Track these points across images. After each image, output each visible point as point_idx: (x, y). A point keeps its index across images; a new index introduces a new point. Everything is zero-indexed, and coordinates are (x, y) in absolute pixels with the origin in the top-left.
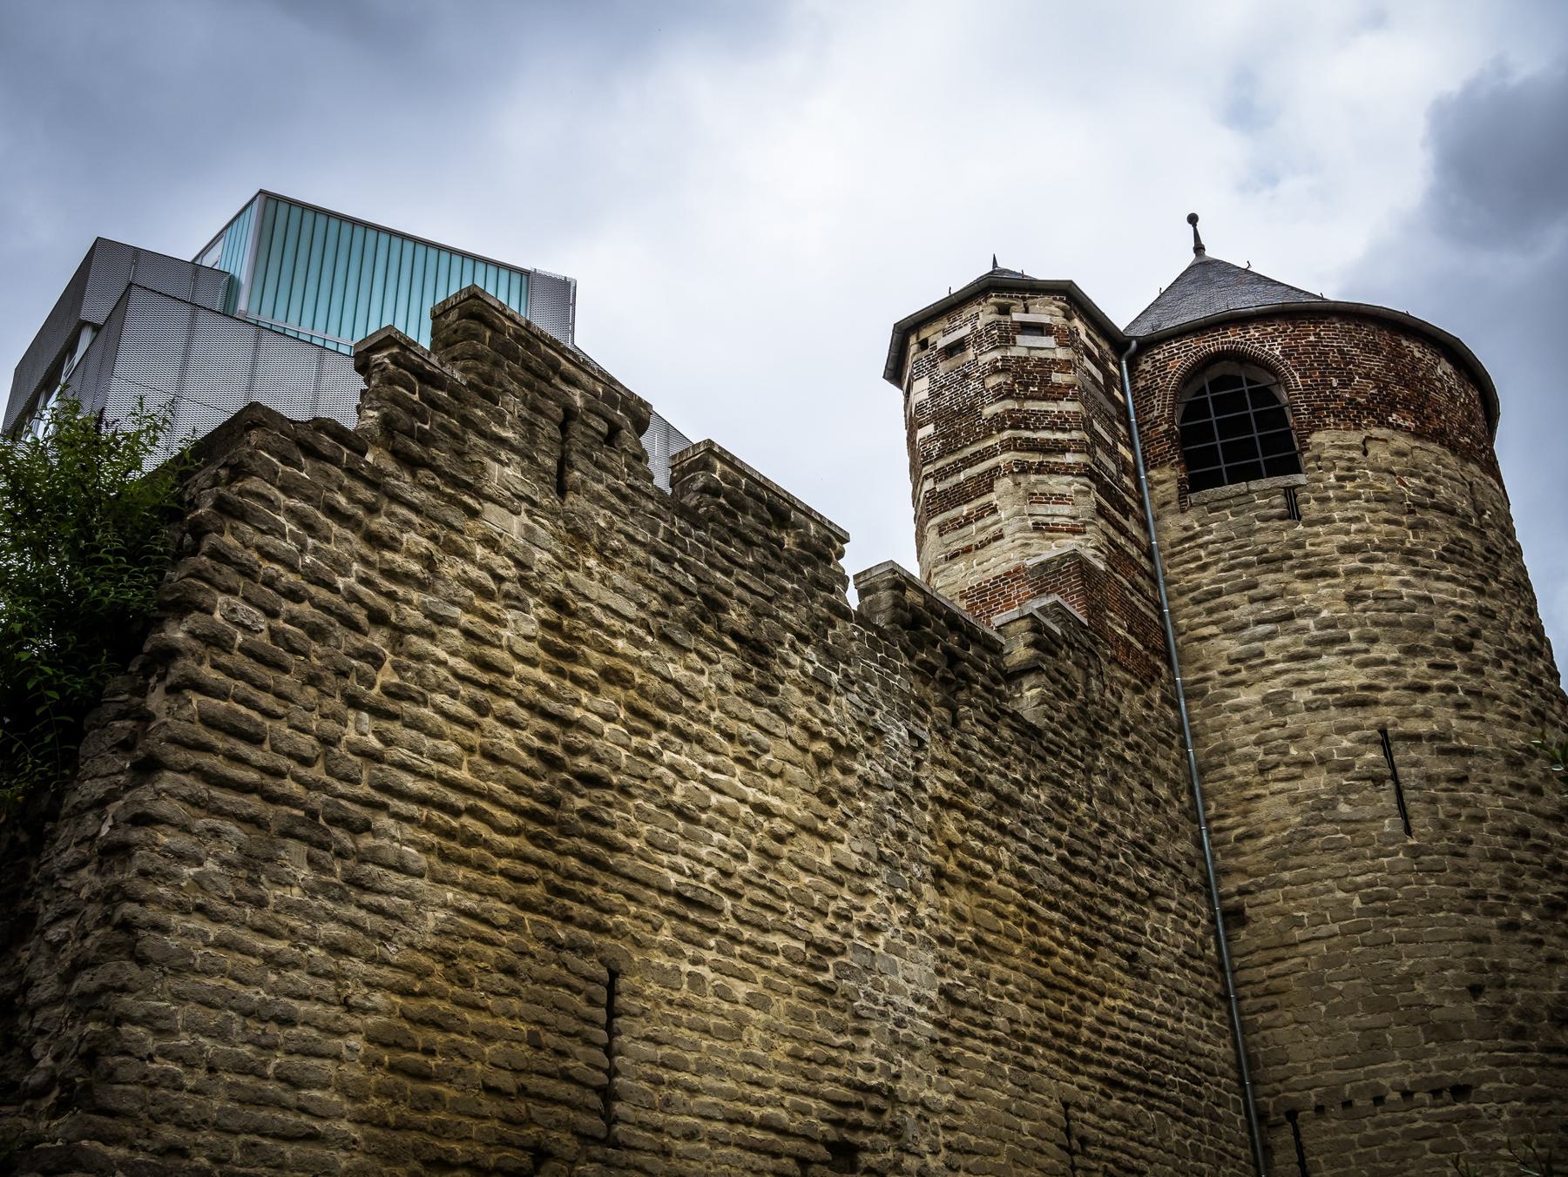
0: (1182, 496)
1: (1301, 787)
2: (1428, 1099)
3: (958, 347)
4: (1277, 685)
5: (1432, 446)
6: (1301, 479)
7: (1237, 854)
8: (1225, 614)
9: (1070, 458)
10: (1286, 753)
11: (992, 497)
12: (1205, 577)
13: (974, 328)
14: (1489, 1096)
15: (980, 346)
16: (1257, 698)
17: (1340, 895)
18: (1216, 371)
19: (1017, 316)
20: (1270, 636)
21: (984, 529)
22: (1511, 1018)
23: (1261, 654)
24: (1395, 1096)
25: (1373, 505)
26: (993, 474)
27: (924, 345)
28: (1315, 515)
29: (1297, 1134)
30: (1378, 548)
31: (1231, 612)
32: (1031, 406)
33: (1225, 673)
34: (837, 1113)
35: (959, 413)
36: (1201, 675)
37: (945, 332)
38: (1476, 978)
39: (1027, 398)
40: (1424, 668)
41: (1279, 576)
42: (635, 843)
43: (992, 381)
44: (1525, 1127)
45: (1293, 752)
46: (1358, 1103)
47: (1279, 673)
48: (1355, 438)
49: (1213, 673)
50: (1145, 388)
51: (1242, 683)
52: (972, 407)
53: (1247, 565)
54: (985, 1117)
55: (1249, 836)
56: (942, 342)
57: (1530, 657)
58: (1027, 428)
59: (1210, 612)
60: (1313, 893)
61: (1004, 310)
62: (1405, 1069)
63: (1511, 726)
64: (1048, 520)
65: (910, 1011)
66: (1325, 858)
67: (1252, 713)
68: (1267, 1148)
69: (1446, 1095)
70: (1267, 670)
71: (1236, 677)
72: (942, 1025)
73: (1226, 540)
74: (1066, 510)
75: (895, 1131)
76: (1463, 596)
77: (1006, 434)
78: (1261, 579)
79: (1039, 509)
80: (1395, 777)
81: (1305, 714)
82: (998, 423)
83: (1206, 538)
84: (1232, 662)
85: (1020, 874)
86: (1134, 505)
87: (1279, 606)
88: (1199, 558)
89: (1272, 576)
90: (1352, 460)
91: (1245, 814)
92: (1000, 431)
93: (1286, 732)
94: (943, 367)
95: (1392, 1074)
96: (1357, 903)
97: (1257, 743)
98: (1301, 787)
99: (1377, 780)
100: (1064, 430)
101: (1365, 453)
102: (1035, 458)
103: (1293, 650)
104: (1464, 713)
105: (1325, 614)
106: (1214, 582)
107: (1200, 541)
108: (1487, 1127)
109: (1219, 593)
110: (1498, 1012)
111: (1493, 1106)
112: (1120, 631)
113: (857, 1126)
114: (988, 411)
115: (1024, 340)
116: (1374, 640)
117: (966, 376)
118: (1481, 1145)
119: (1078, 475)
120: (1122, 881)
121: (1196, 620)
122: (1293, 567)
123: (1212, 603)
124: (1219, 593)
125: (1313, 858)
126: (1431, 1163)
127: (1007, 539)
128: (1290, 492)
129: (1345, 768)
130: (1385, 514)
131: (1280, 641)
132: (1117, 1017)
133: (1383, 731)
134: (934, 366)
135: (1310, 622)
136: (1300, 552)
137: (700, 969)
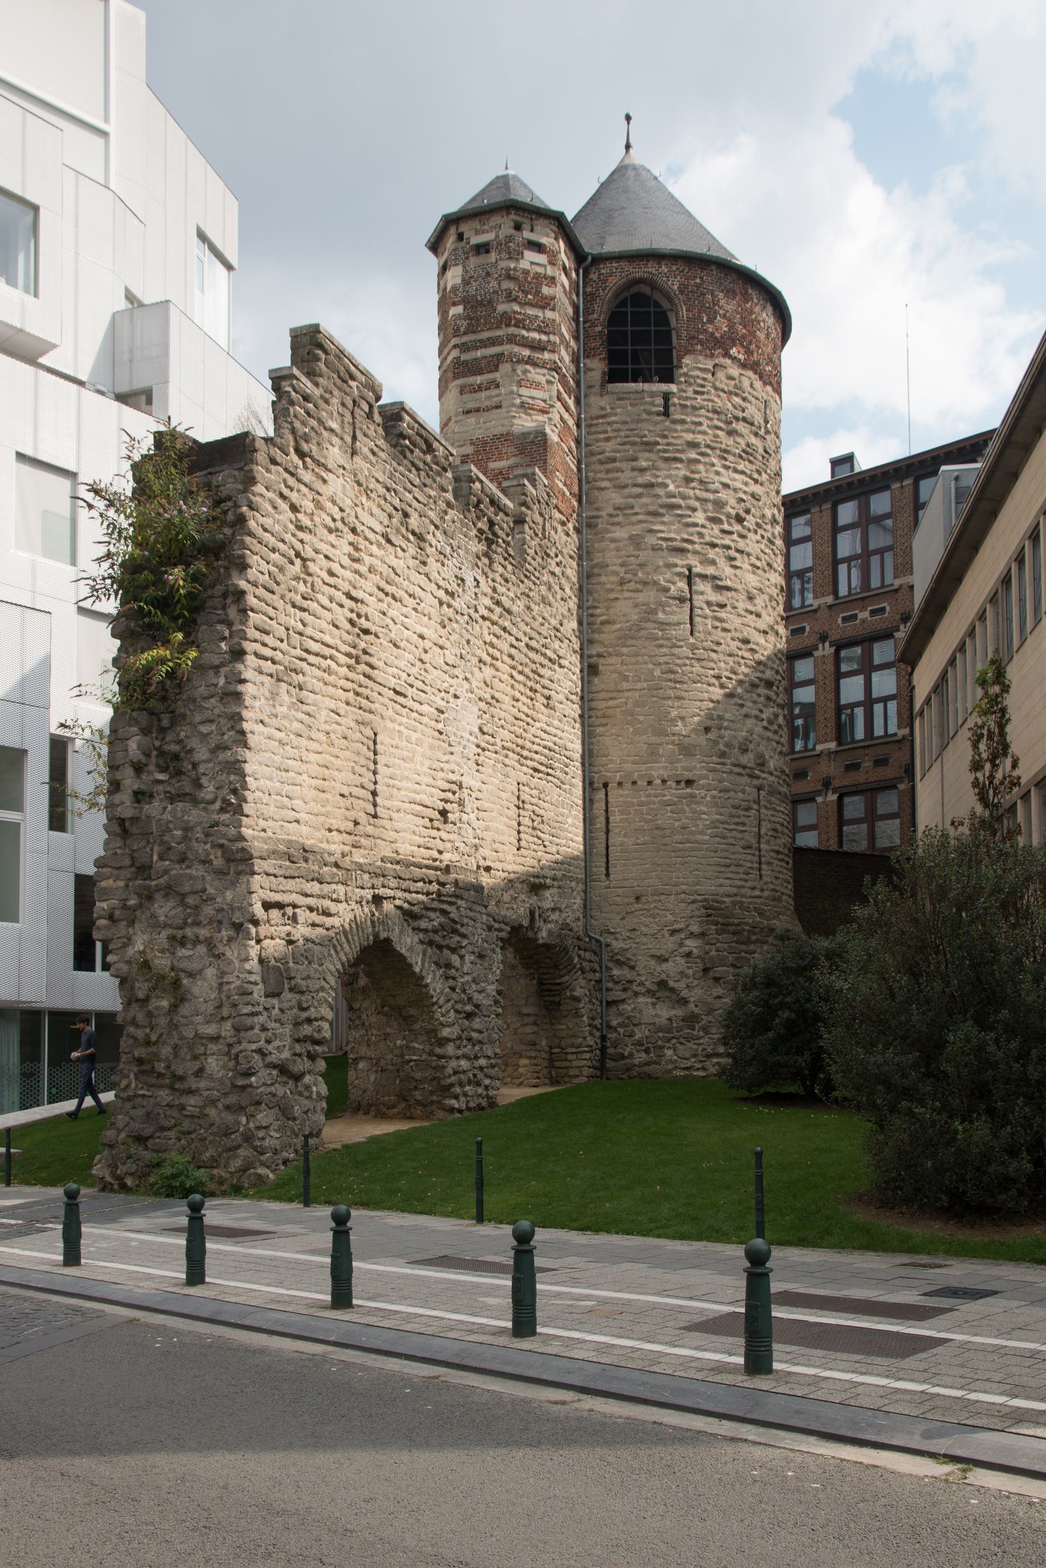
0: (603, 386)
1: (641, 598)
2: (674, 785)
3: (483, 249)
4: (636, 530)
8: (616, 475)
9: (547, 356)
10: (636, 575)
11: (497, 376)
12: (609, 446)
13: (497, 236)
14: (703, 787)
15: (500, 253)
16: (626, 535)
17: (651, 666)
18: (635, 289)
19: (527, 234)
20: (639, 496)
21: (489, 398)
22: (721, 747)
23: (632, 507)
24: (659, 781)
26: (499, 357)
31: (620, 474)
32: (531, 311)
33: (610, 515)
34: (443, 795)
35: (481, 304)
36: (595, 513)
37: (477, 232)
38: (709, 723)
39: (526, 304)
41: (650, 455)
43: (506, 285)
44: (716, 805)
45: (640, 575)
47: (641, 522)
49: (603, 513)
50: (591, 294)
51: (618, 524)
52: (490, 302)
53: (633, 444)
55: (607, 622)
58: (524, 328)
59: (608, 471)
60: (637, 663)
61: (518, 227)
62: (666, 768)
66: (647, 643)
67: (621, 544)
68: (591, 800)
69: (683, 784)
70: (634, 519)
71: (616, 520)
72: (478, 746)
73: (624, 423)
75: (461, 803)
77: (512, 330)
78: (640, 455)
79: (524, 391)
80: (691, 600)
81: (650, 552)
82: (507, 319)
83: (613, 419)
84: (616, 509)
85: (510, 656)
87: (647, 478)
88: (606, 432)
89: (647, 455)
91: (608, 608)
92: (508, 325)
93: (638, 561)
94: (474, 261)
95: (659, 770)
96: (657, 673)
97: (622, 565)
98: (641, 598)
100: (545, 333)
102: (526, 352)
103: (651, 508)
105: (671, 487)
106: (613, 451)
107: (610, 420)
108: (699, 803)
109: (614, 460)
110: (715, 742)
111: (703, 792)
112: (561, 485)
113: (446, 801)
114: (501, 308)
115: (530, 256)
117: (488, 274)
118: (694, 812)
119: (550, 369)
120: (548, 652)
121: (599, 475)
122: (659, 451)
123: (610, 466)
124: (614, 460)
125: (639, 643)
126: (669, 818)
127: (504, 410)
131: (644, 500)
133: (690, 570)
136: (665, 441)
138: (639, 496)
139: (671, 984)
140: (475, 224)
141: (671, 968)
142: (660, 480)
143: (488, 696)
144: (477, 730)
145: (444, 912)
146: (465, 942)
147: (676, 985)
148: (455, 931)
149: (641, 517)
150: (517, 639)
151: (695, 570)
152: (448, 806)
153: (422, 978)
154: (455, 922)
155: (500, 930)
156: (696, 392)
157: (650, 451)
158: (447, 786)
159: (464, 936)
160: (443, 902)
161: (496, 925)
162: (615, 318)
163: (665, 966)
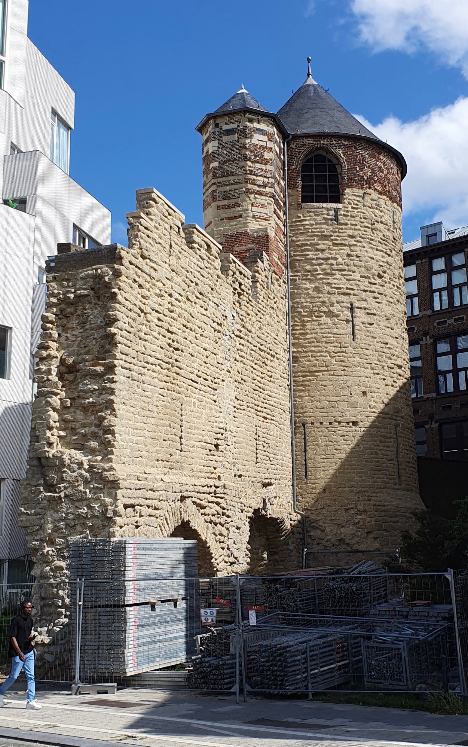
5: (385, 197)
6: (340, 206)
7: (298, 339)
8: (307, 253)
13: (238, 126)
25: (363, 220)
27: (217, 125)
28: (342, 221)
29: (304, 430)
30: (361, 237)
32: (258, 166)
37: (227, 123)
39: (255, 162)
40: (367, 283)
42: (185, 366)
46: (324, 423)
48: (361, 192)
54: (241, 432)
56: (225, 127)
57: (399, 279)
58: (254, 175)
60: (321, 356)
63: (389, 305)
64: (259, 214)
65: (230, 404)
69: (351, 424)
70: (318, 277)
72: (235, 407)
74: (264, 210)
76: (383, 257)
80: (353, 321)
86: (282, 204)
87: (326, 255)
90: (358, 201)
94: (225, 139)
97: (311, 302)
99: (347, 321)
101: (363, 198)
104: (377, 300)
112: (276, 259)
116: (353, 272)
119: (270, 197)
122: (332, 240)
128: (336, 210)
129: (337, 316)
130: (366, 224)
131: (324, 267)
132: (267, 397)
133: (352, 305)
134: (221, 137)
135: (334, 262)
137: (195, 400)
138: (320, 264)
139: (347, 541)
140: (227, 119)
141: (347, 531)
142: (333, 256)
143: (239, 379)
144: (234, 398)
145: (218, 504)
146: (230, 520)
147: (350, 541)
148: (224, 514)
149: (322, 276)
150: (254, 346)
151: (355, 305)
152: (219, 442)
153: (206, 542)
154: (224, 509)
155: (248, 512)
156: (353, 208)
157: (328, 240)
158: (219, 431)
159: (228, 516)
160: (217, 497)
161: (246, 509)
162: (306, 168)
163: (342, 529)
